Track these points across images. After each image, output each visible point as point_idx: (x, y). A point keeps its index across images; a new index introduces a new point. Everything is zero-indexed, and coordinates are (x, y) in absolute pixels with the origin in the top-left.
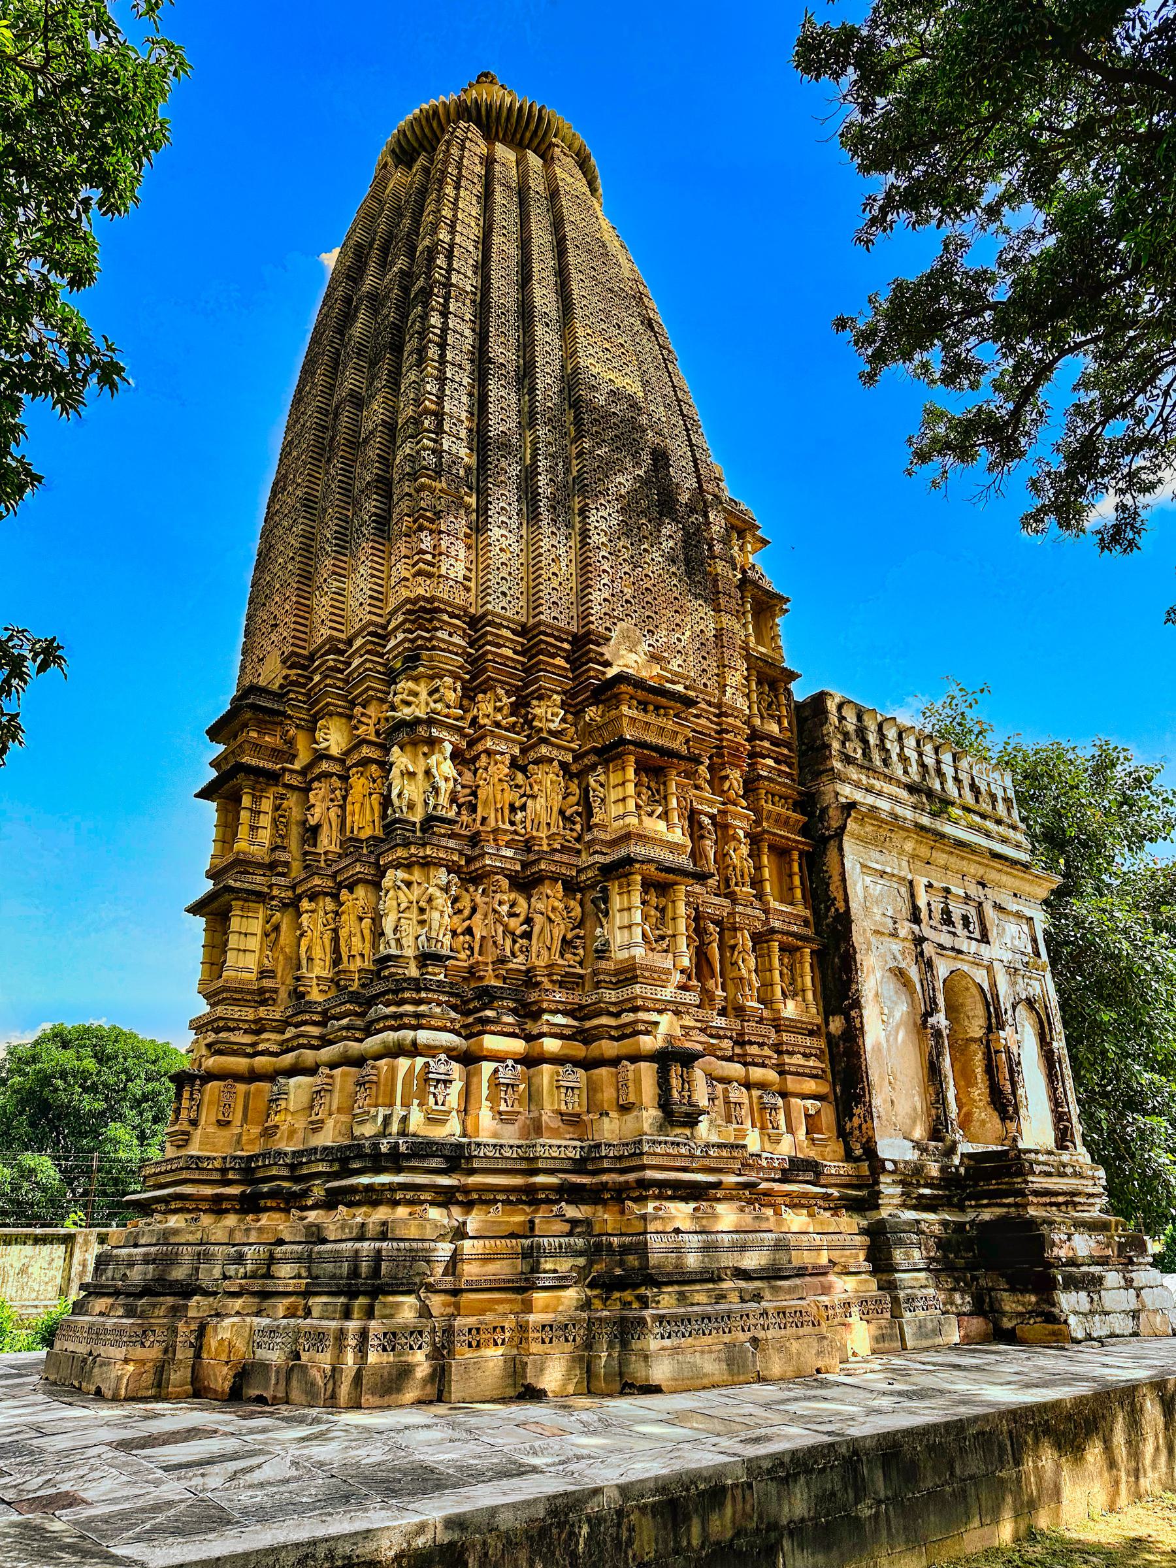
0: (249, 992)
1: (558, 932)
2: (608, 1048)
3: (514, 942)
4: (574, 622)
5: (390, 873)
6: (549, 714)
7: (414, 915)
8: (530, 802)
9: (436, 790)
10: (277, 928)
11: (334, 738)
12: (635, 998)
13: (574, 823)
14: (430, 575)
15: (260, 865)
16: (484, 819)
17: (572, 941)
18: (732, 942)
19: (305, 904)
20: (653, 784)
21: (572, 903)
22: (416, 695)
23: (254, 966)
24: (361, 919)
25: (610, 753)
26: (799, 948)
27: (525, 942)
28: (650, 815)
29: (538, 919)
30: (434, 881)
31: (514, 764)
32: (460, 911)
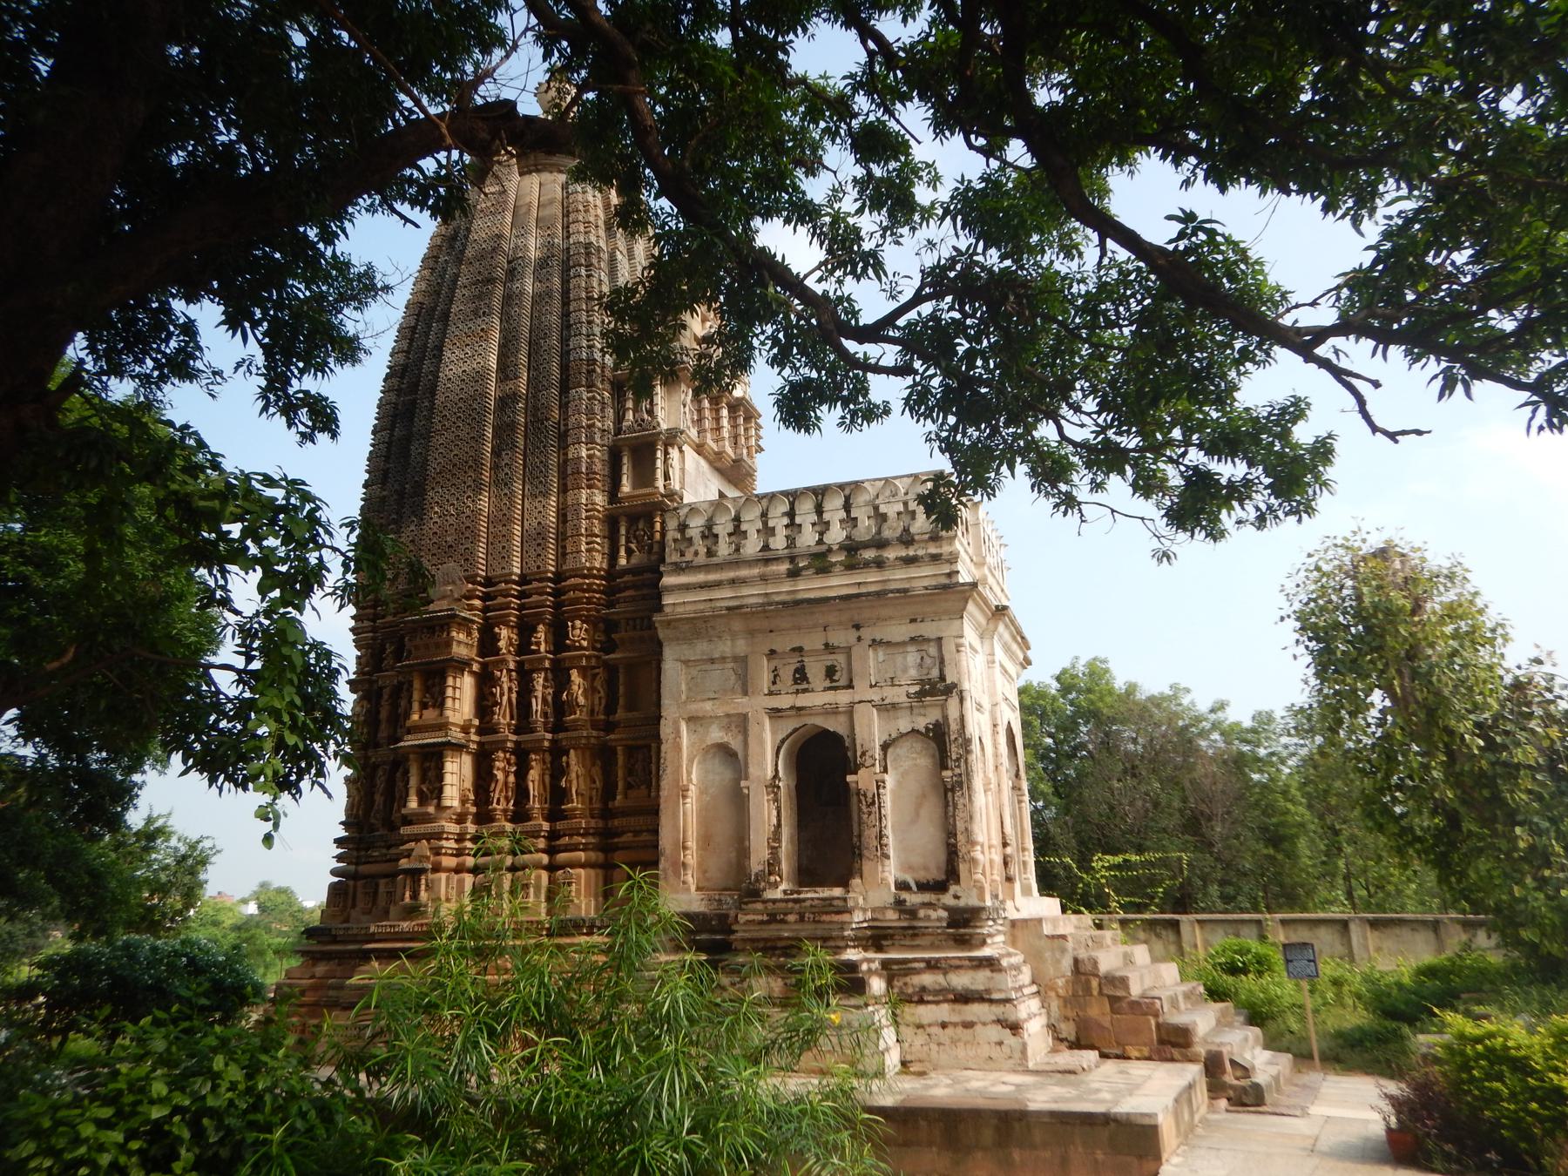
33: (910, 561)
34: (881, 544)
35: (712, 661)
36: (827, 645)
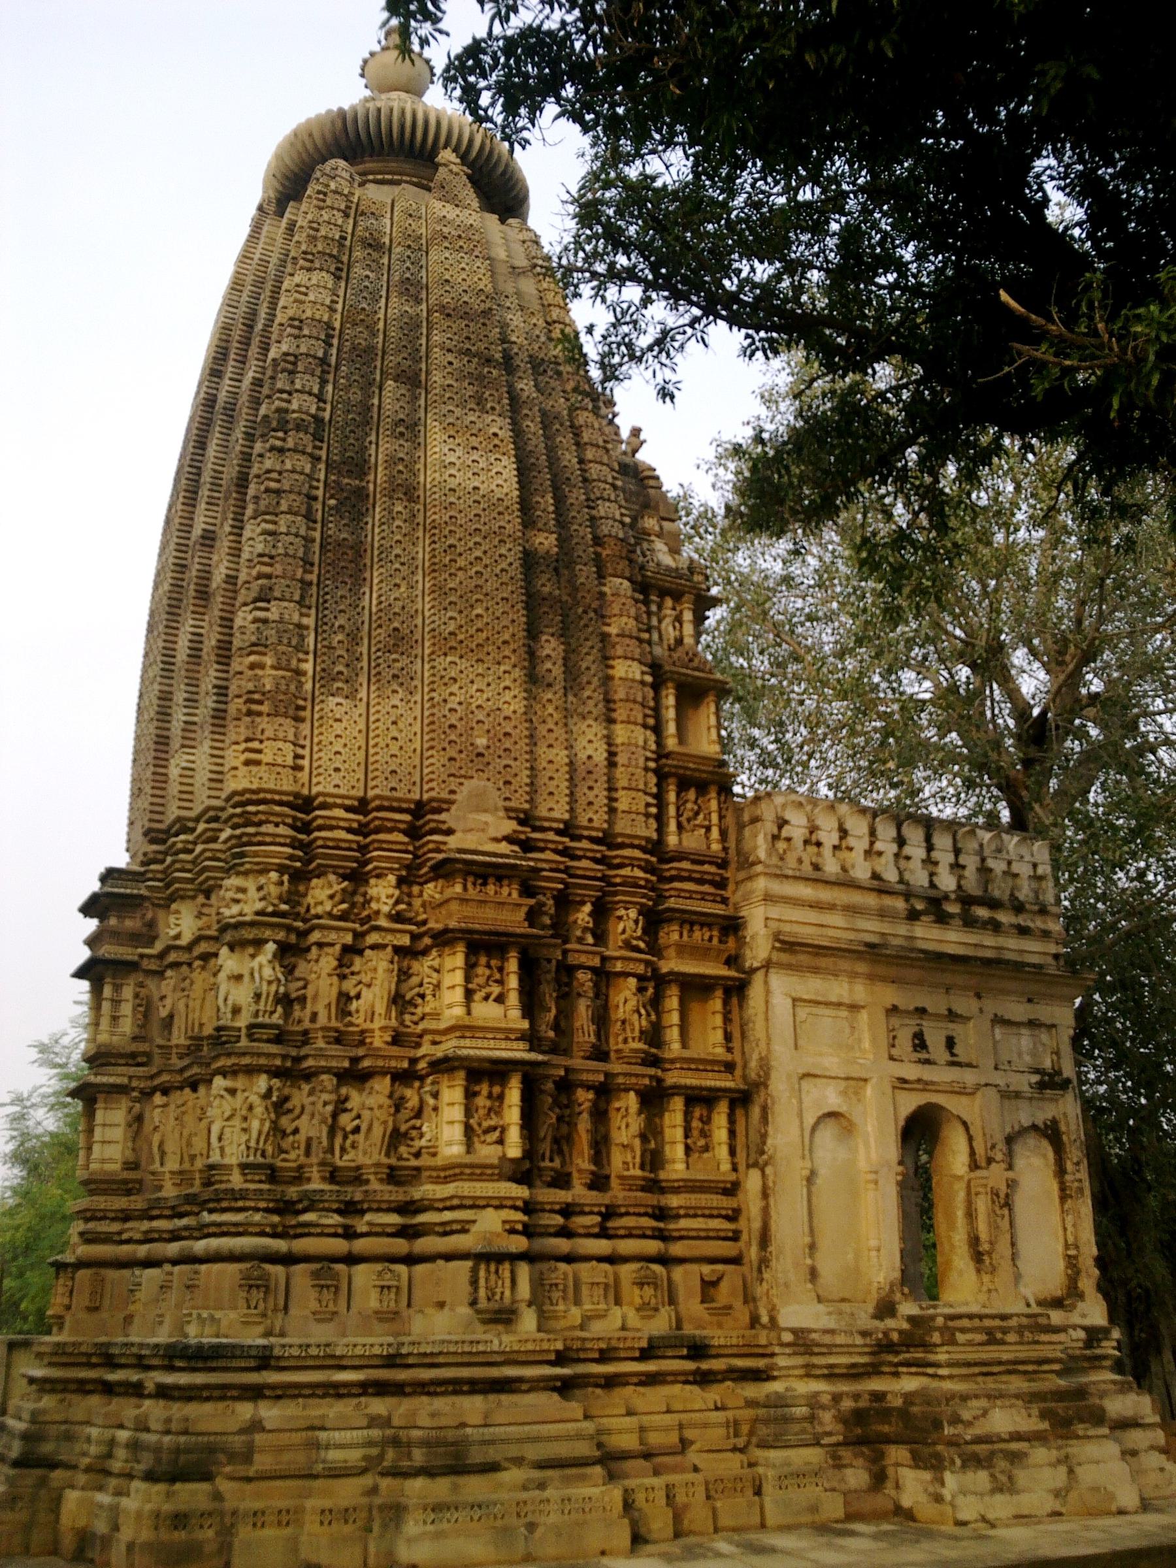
0: (114, 1182)
2: (425, 1244)
3: (345, 1137)
4: (417, 789)
6: (383, 893)
7: (237, 1122)
8: (365, 993)
13: (416, 1006)
14: (258, 763)
15: (121, 1056)
17: (406, 1134)
18: (617, 1105)
19: (158, 1099)
20: (493, 963)
22: (243, 890)
23: (118, 1156)
25: (443, 939)
28: (486, 998)
29: (366, 1114)
30: (255, 1089)
32: (290, 1111)
33: (1023, 931)
34: (994, 904)
35: (827, 1004)
36: (950, 1010)
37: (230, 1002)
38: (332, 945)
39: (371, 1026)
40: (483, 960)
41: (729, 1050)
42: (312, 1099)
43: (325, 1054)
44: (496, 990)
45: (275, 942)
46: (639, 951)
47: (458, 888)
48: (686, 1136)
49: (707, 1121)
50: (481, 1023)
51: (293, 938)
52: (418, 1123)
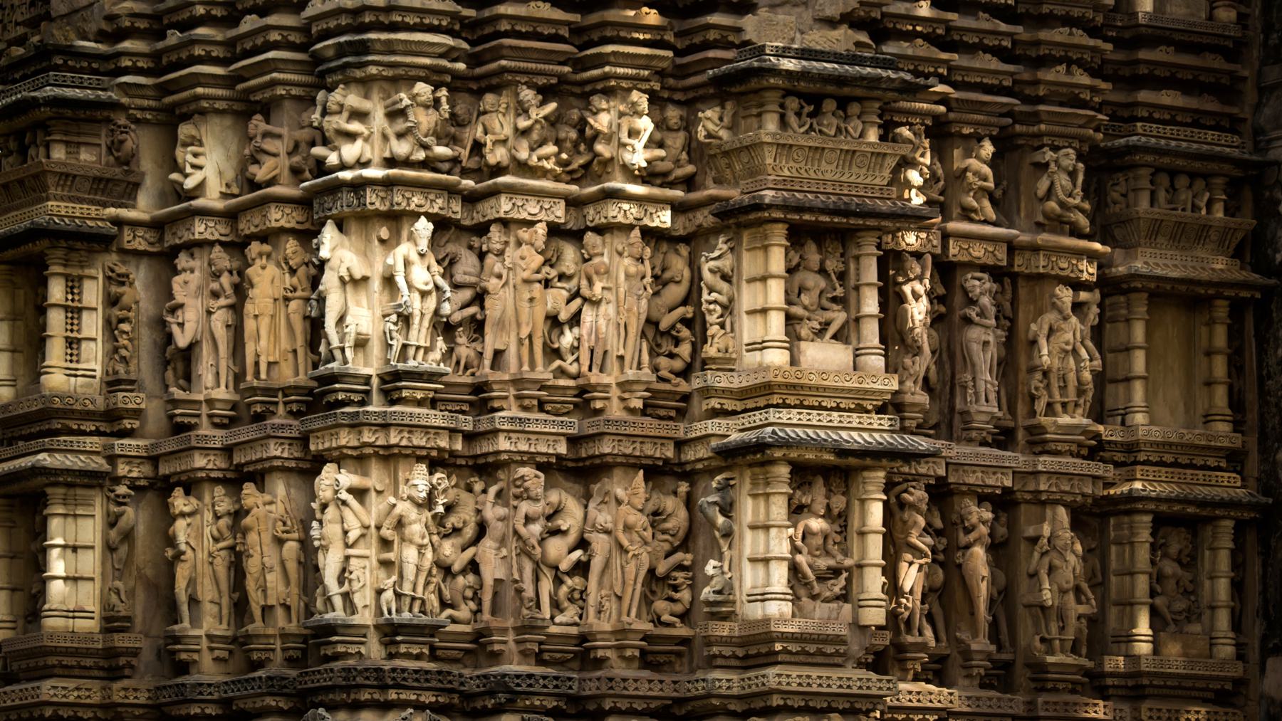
0: (88, 653)
1: (635, 570)
3: (558, 581)
5: (329, 471)
7: (371, 550)
8: (588, 315)
9: (405, 320)
10: (128, 536)
11: (209, 166)
12: (771, 692)
13: (677, 341)
15: (88, 415)
16: (498, 354)
17: (667, 577)
18: (1030, 531)
19: (180, 502)
20: (832, 265)
21: (670, 503)
24: (280, 542)
25: (739, 220)
26: (1212, 520)
27: (576, 582)
28: (820, 333)
29: (600, 543)
30: (404, 490)
31: (555, 231)
32: (456, 531)
37: (351, 330)
38: (531, 224)
39: (605, 379)
40: (814, 257)
41: (1238, 426)
42: (501, 511)
43: (522, 433)
44: (838, 317)
45: (429, 217)
46: (1076, 232)
47: (771, 124)
48: (1153, 593)
49: (1189, 561)
50: (815, 380)
51: (456, 209)
52: (687, 558)
